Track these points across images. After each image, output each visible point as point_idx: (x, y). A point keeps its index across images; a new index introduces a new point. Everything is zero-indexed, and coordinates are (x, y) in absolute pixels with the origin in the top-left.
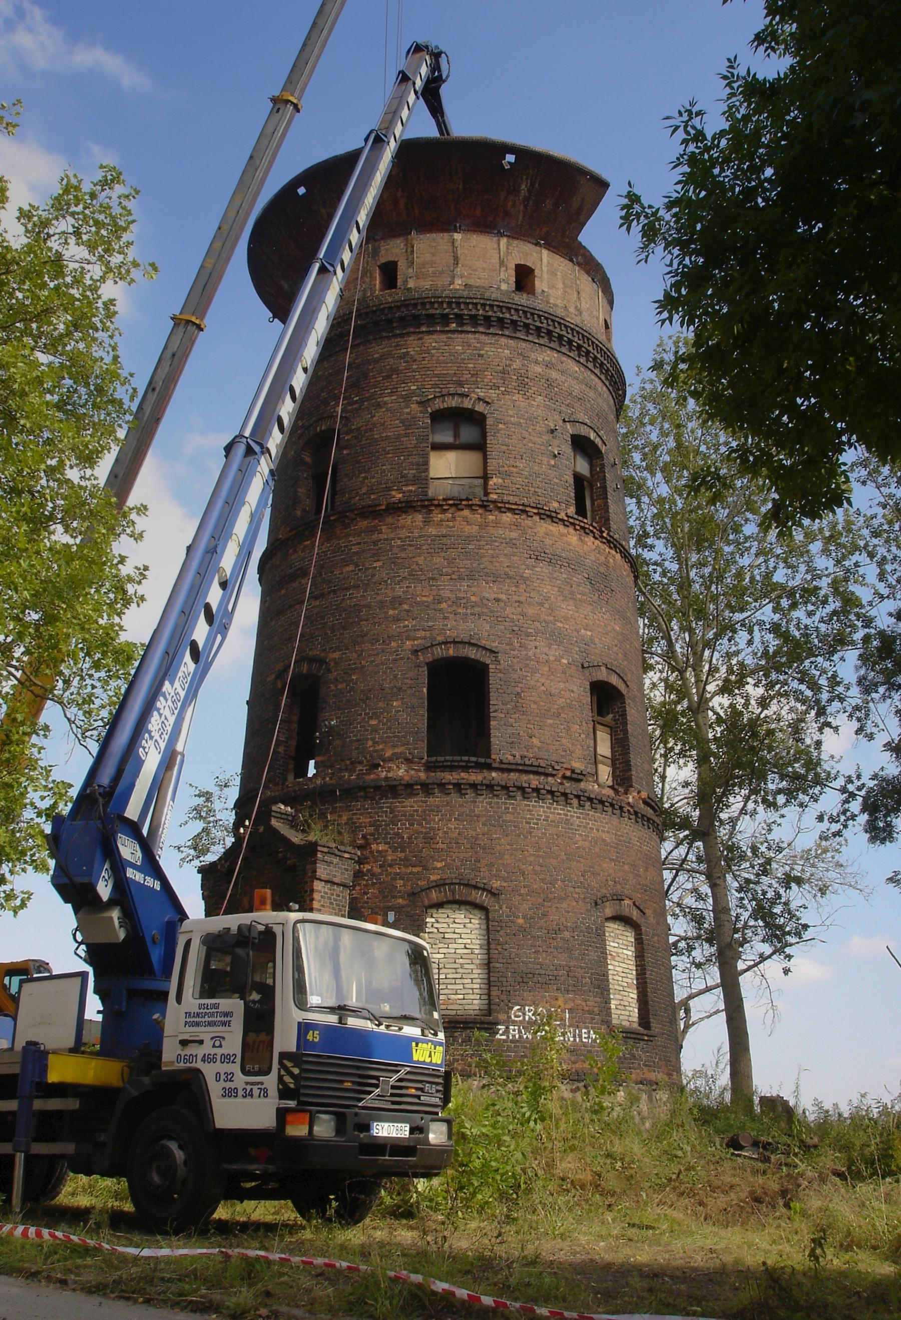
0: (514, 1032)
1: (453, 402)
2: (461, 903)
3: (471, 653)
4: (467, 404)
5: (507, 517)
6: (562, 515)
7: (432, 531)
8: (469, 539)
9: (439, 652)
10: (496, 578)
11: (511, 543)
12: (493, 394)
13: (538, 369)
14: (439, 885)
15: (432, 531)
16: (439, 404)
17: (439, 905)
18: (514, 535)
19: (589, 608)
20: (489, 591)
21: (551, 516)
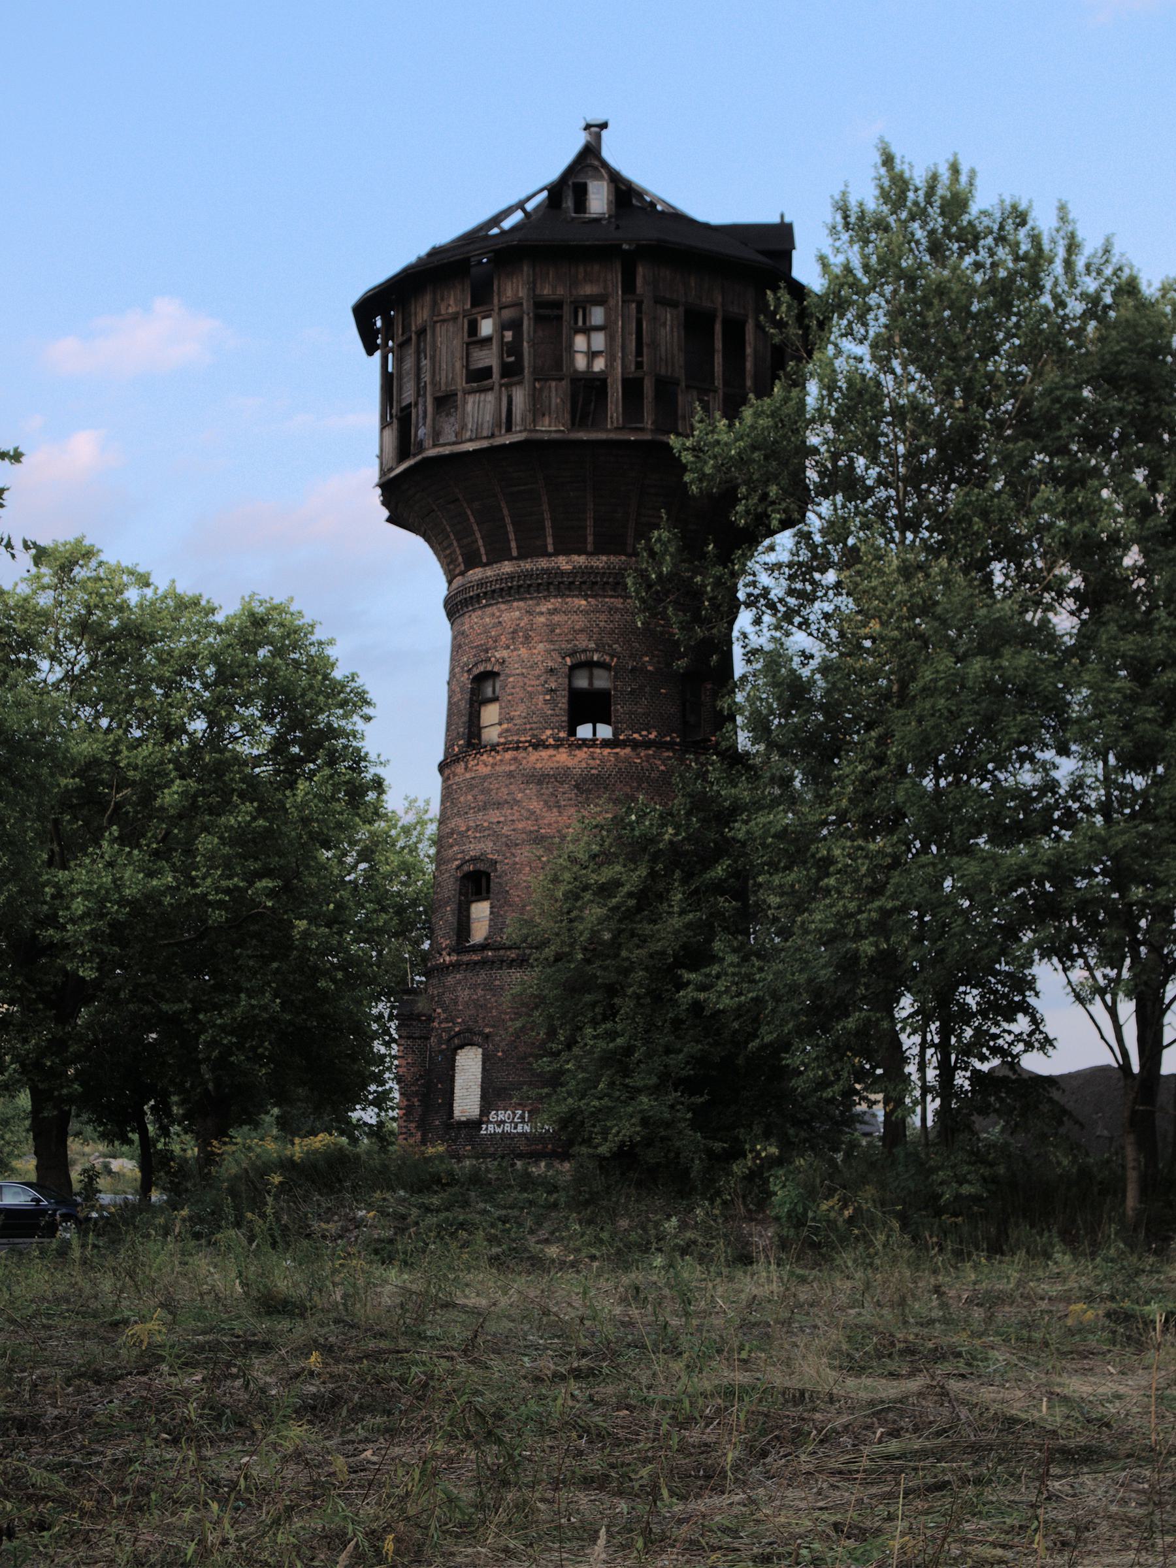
0: (491, 1128)
1: (481, 668)
2: (472, 1045)
3: (481, 866)
4: (489, 668)
5: (509, 755)
6: (551, 741)
7: (468, 776)
8: (485, 778)
9: (465, 868)
10: (499, 805)
11: (510, 775)
12: (505, 653)
13: (542, 619)
14: (458, 1034)
15: (468, 776)
16: (476, 671)
17: (461, 1047)
18: (512, 768)
19: (572, 810)
20: (494, 816)
21: (539, 745)
